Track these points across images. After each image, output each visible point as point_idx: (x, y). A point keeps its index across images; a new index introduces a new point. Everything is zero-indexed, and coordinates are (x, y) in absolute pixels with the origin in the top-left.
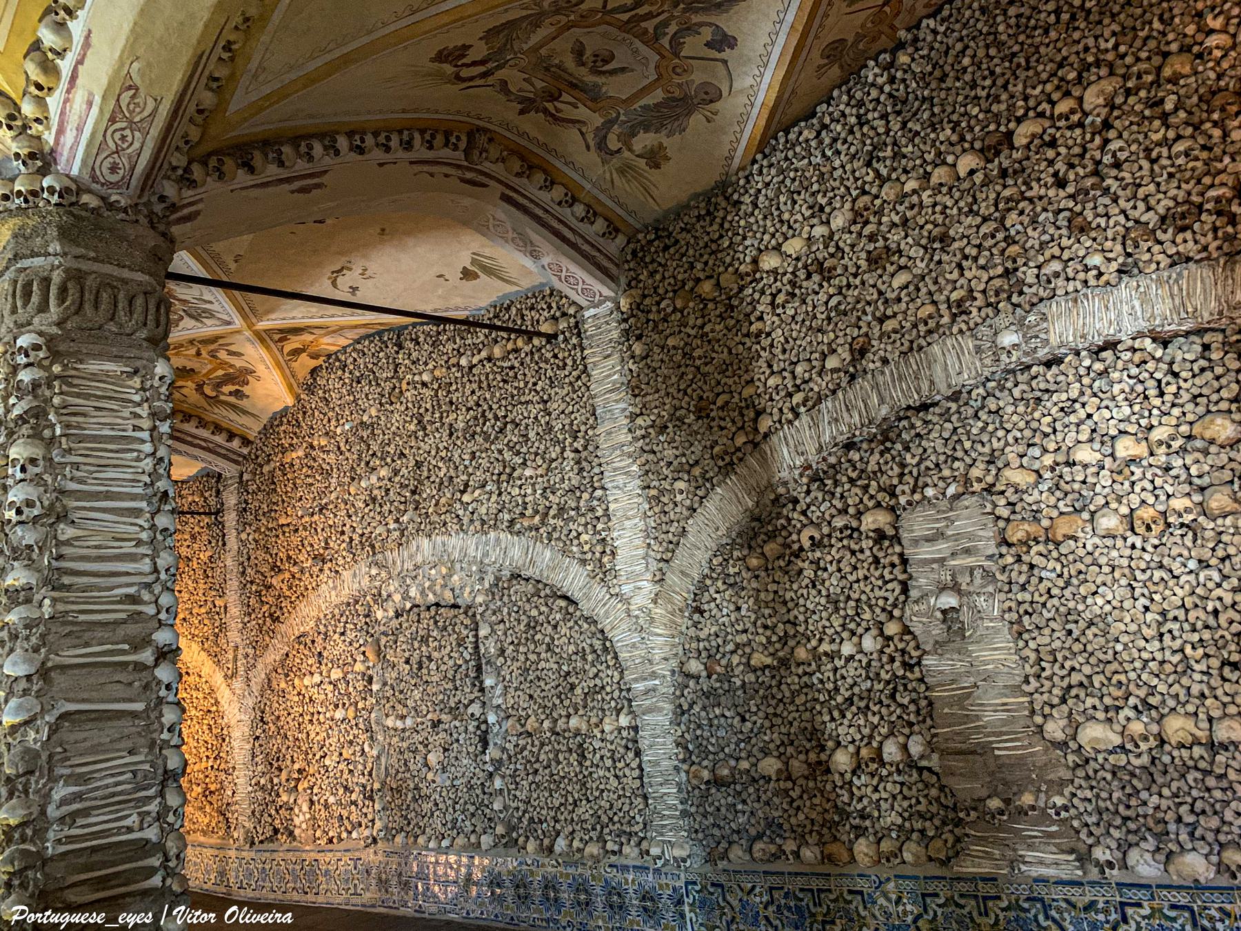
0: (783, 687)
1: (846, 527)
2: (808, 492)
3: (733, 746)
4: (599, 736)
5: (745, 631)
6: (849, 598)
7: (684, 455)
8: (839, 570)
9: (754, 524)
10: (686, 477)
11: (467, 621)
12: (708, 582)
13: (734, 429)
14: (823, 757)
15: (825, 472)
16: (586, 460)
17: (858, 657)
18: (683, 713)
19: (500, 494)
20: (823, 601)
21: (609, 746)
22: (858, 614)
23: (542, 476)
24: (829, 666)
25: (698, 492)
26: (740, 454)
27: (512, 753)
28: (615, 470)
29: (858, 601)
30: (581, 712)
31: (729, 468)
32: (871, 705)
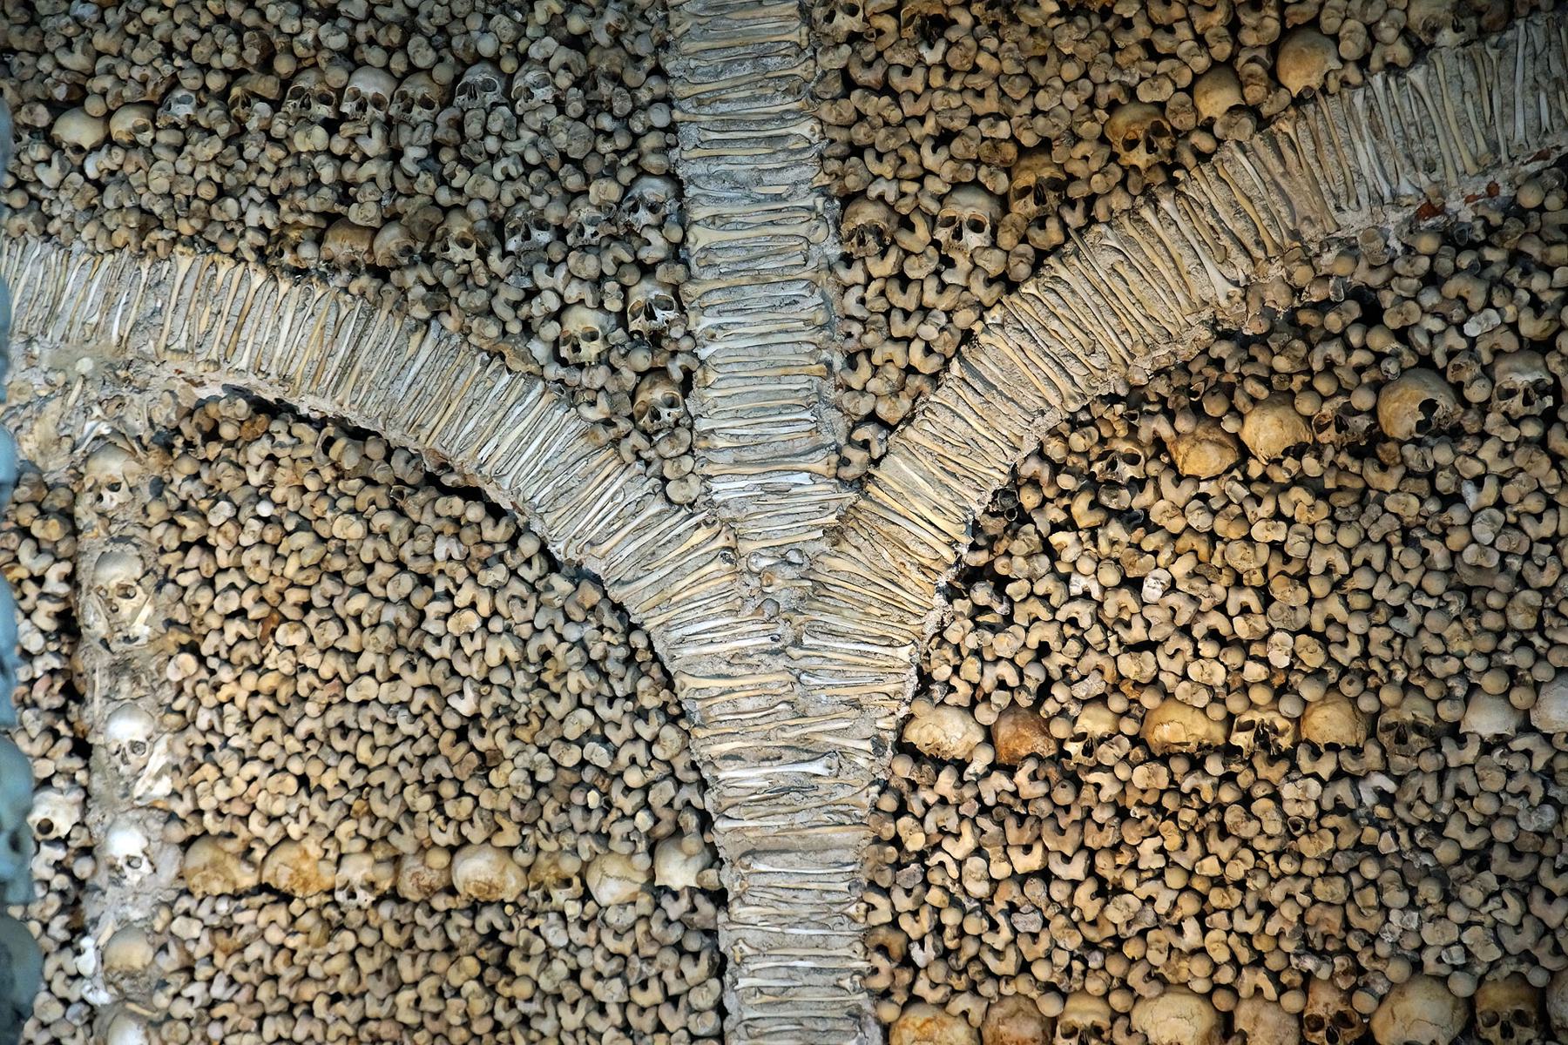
0: (1262, 806)
1: (1539, 389)
2: (1432, 279)
3: (1061, 959)
4: (573, 909)
5: (1151, 646)
6: (1522, 581)
7: (1008, 118)
8: (1501, 504)
9: (1222, 349)
10: (1001, 184)
11: (51, 530)
12: (1029, 499)
13: (1201, 62)
14: (1363, 1002)
15: (1489, 228)
16: (617, 79)
17: (1519, 744)
18: (898, 866)
19: (237, 137)
20: (1435, 584)
21: (611, 943)
22: (1540, 628)
23: (426, 103)
24: (1429, 762)
25: (1034, 233)
26: (1204, 143)
27: (199, 952)
28: (728, 122)
29: (1545, 591)
30: (509, 836)
31: (1160, 178)
32: (1545, 873)
